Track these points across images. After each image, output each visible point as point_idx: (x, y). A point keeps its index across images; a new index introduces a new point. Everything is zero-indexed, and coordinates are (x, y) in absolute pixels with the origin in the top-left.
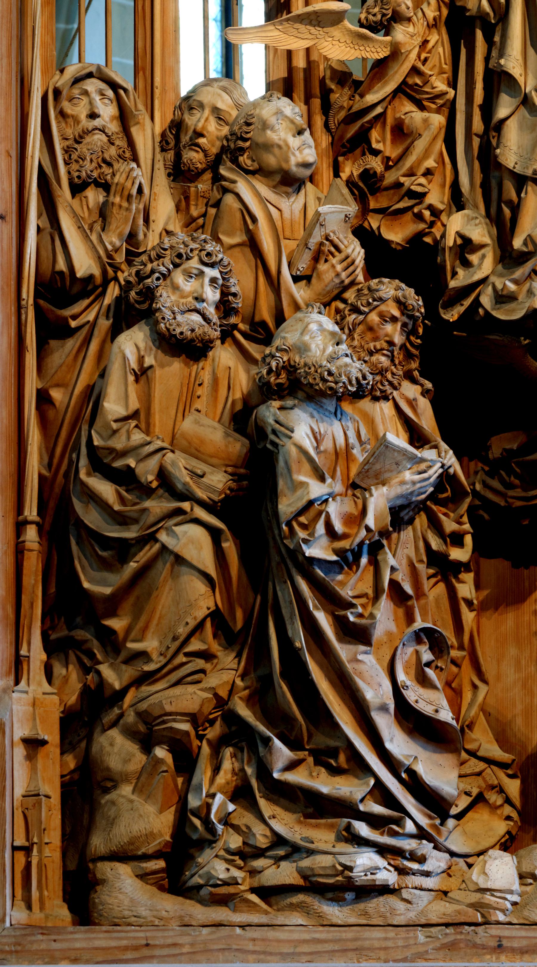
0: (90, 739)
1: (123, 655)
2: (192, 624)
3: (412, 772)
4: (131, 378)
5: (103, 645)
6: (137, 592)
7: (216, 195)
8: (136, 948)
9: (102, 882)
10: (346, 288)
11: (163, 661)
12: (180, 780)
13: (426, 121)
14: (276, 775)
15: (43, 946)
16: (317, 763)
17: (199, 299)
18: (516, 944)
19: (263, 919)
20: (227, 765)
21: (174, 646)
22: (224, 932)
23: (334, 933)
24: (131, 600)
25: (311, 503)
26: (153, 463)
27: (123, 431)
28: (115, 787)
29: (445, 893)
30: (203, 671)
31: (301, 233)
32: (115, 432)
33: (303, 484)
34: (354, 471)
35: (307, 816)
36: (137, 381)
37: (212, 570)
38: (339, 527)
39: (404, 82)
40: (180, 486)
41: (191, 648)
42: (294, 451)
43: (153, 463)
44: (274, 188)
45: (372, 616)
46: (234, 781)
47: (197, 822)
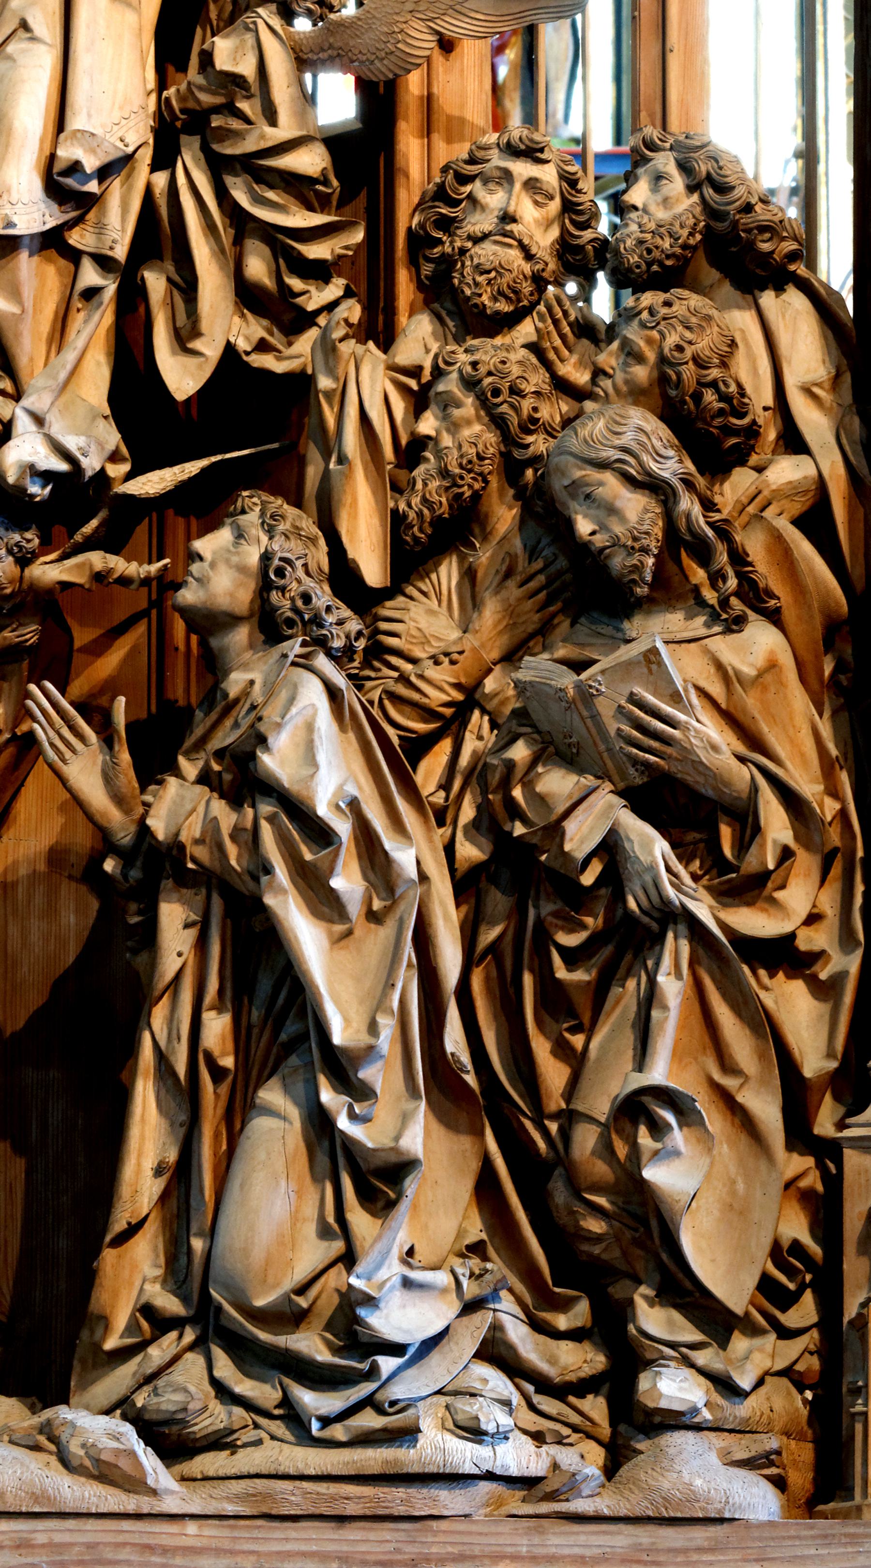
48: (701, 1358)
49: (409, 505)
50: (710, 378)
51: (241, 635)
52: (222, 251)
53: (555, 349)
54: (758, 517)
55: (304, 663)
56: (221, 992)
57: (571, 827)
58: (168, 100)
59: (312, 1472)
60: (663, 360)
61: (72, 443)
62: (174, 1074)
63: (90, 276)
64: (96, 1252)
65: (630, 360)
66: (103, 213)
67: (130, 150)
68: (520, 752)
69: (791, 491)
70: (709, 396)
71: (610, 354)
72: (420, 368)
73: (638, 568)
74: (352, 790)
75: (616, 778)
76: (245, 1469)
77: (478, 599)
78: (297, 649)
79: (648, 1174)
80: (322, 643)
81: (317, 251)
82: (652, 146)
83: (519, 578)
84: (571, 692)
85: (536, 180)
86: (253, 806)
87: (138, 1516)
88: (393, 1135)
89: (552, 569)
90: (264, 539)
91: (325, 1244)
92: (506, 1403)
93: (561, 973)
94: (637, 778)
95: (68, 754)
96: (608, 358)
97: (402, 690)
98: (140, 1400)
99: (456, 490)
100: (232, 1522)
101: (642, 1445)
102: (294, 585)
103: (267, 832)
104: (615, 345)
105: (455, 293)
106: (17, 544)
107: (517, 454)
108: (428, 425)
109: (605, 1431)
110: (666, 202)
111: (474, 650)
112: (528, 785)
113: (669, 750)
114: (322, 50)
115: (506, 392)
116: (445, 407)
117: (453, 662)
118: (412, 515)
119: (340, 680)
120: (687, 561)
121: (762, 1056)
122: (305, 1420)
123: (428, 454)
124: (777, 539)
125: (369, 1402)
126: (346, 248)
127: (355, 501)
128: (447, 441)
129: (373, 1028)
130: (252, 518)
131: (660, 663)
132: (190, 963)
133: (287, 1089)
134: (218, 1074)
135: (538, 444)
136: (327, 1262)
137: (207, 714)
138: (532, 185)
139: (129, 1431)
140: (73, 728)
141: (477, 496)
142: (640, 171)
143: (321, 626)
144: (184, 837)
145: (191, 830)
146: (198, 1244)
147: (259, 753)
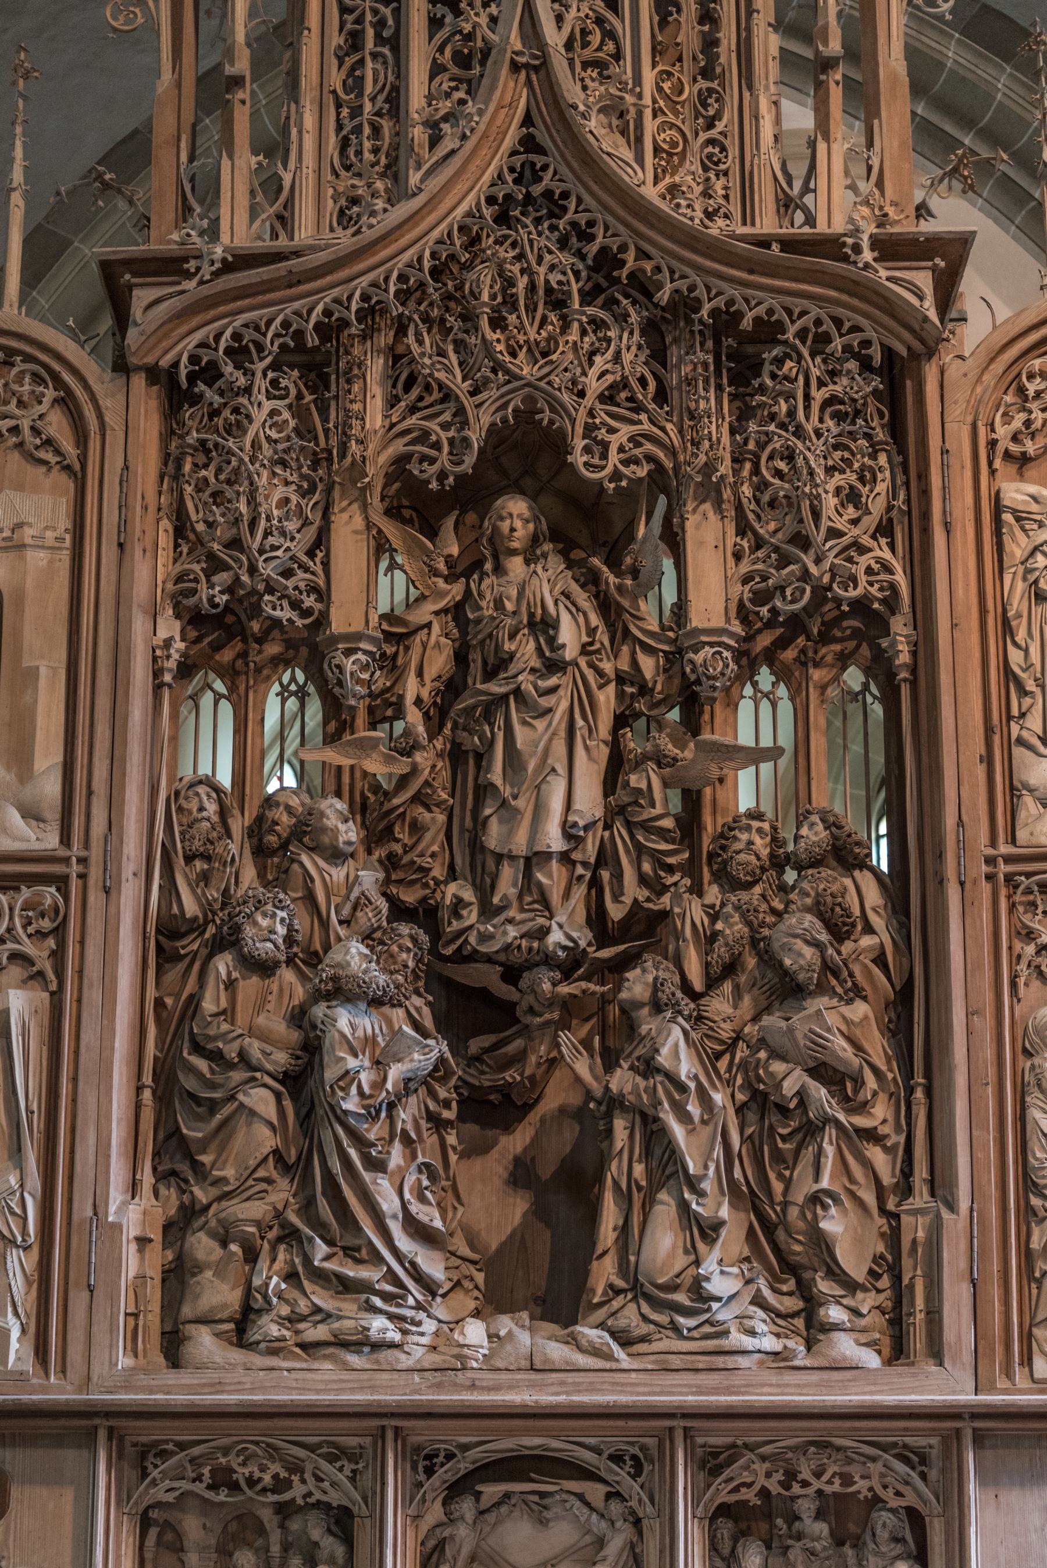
0: (183, 1239)
1: (210, 1180)
2: (260, 1158)
3: (413, 1264)
4: (222, 986)
5: (195, 1172)
6: (221, 1136)
7: (286, 864)
8: (212, 1385)
9: (189, 1338)
10: (374, 931)
11: (238, 1184)
12: (247, 1268)
13: (433, 819)
14: (316, 1263)
15: (145, 1383)
16: (346, 1255)
17: (272, 932)
18: (485, 1384)
19: (304, 1365)
20: (281, 1256)
21: (246, 1174)
22: (275, 1374)
23: (355, 1375)
24: (217, 1142)
25: (347, 1072)
26: (236, 1045)
27: (215, 1023)
28: (200, 1272)
29: (435, 1348)
30: (266, 1191)
31: (343, 892)
32: (210, 1023)
33: (342, 1059)
34: (378, 1052)
35: (338, 1293)
36: (226, 989)
37: (275, 1121)
38: (367, 1089)
39: (419, 791)
40: (254, 1061)
41: (257, 1175)
42: (337, 1035)
43: (236, 1045)
44: (326, 860)
45: (389, 1153)
46: (287, 1269)
47: (258, 1296)
48: (845, 1301)
51: (645, 1011)
54: (857, 959)
55: (673, 1020)
57: (786, 1084)
60: (818, 894)
61: (575, 935)
62: (621, 1189)
63: (580, 870)
66: (585, 845)
68: (762, 1055)
69: (870, 949)
70: (838, 909)
73: (810, 978)
74: (693, 1070)
79: (821, 1225)
80: (680, 1012)
82: (809, 812)
87: (611, 1370)
92: (764, 1321)
93: (780, 1145)
94: (812, 1064)
96: (793, 896)
97: (710, 1033)
101: (821, 1337)
105: (728, 875)
107: (757, 936)
108: (719, 926)
109: (805, 1334)
112: (766, 1069)
119: (688, 1027)
121: (867, 1176)
124: (866, 966)
125: (707, 1321)
128: (728, 932)
129: (706, 1167)
130: (650, 963)
134: (639, 1188)
135: (766, 932)
138: (760, 830)
139: (606, 1335)
141: (740, 954)
145: (628, 1088)
146: (632, 1258)
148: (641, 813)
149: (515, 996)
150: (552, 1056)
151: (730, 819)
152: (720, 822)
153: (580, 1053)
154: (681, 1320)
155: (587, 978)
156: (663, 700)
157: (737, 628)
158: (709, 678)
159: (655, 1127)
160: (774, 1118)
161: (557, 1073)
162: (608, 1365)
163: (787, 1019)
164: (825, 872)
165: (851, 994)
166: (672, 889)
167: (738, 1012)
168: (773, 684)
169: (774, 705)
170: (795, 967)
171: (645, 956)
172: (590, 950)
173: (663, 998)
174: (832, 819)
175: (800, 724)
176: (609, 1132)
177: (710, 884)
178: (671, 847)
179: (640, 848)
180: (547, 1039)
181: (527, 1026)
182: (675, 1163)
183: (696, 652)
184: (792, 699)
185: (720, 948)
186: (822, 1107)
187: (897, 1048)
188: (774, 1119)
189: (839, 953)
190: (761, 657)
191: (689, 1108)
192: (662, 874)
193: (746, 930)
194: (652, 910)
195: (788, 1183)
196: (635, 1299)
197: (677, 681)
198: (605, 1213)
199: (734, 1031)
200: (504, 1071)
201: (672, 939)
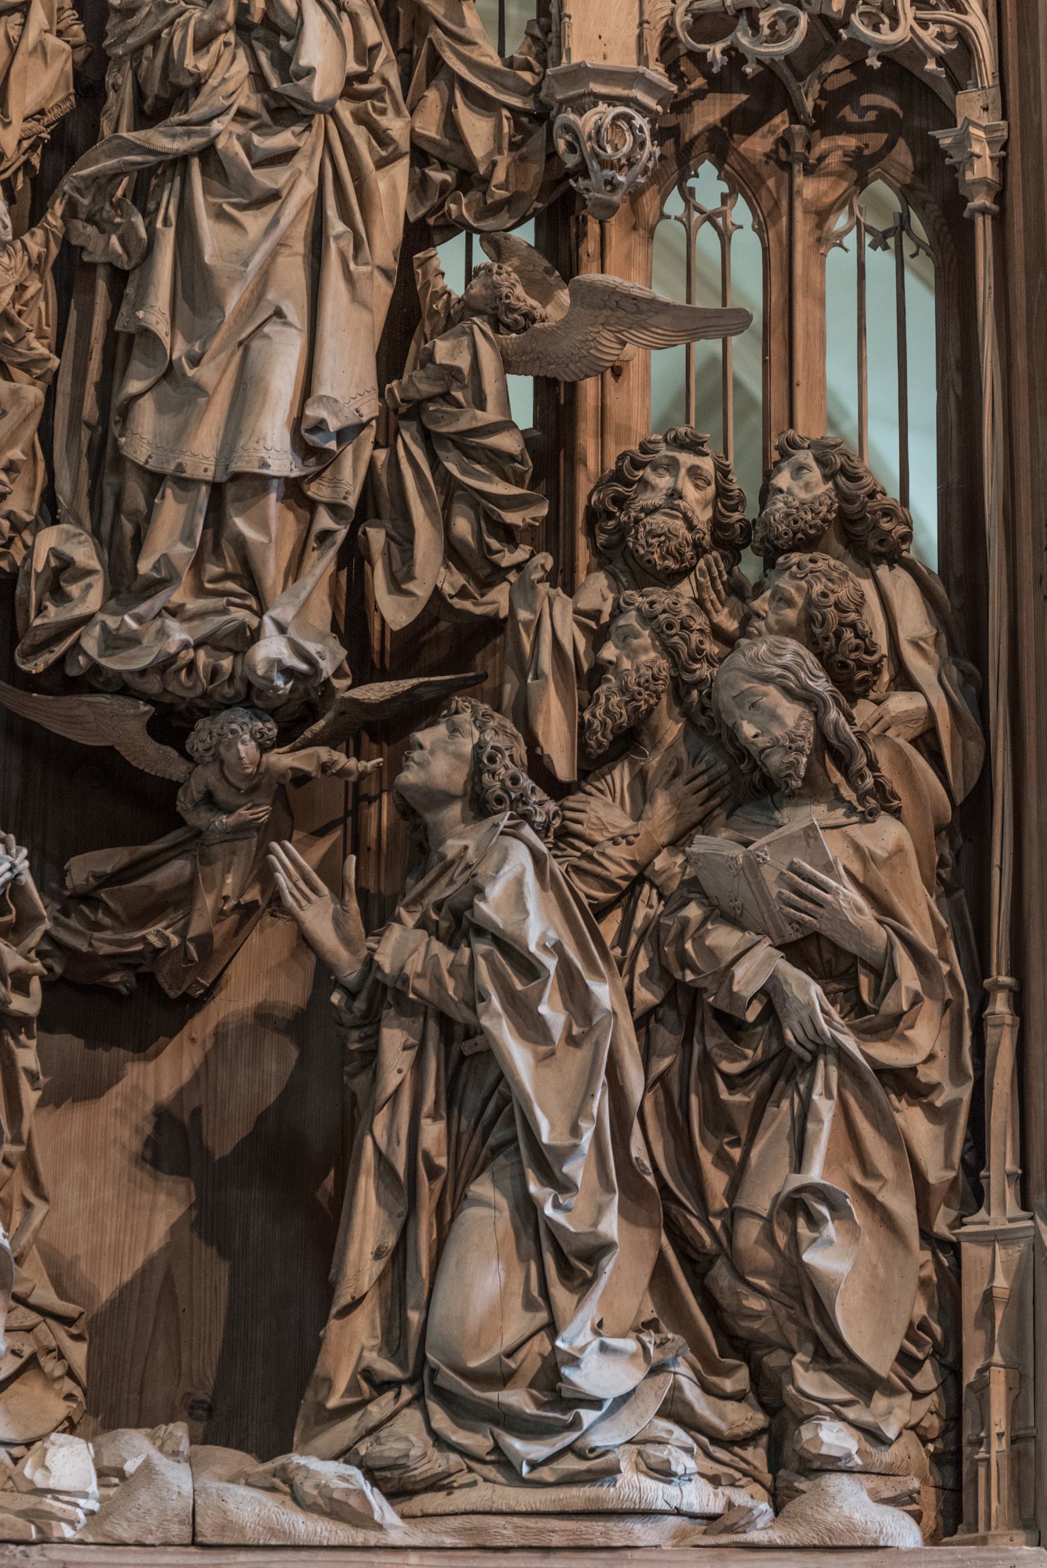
49: (594, 715)
50: (849, 620)
51: (455, 810)
52: (435, 511)
53: (712, 601)
55: (511, 832)
56: (436, 1102)
57: (740, 972)
58: (391, 390)
59: (523, 1509)
61: (312, 648)
64: (324, 1322)
65: (782, 604)
66: (338, 470)
67: (365, 419)
68: (693, 911)
71: (764, 600)
72: (599, 612)
73: (794, 765)
74: (552, 934)
75: (774, 935)
76: (463, 1507)
77: (649, 794)
78: (505, 822)
80: (527, 817)
81: (513, 518)
82: (793, 445)
83: (685, 777)
84: (741, 860)
85: (698, 467)
86: (469, 945)
87: (366, 1548)
88: (590, 1222)
89: (713, 771)
90: (476, 733)
91: (530, 1315)
94: (792, 935)
95: (304, 903)
96: (760, 604)
97: (585, 864)
98: (363, 1449)
99: (634, 703)
100: (449, 1553)
102: (502, 770)
103: (482, 965)
104: (768, 594)
106: (260, 731)
107: (686, 677)
108: (609, 652)
110: (807, 486)
111: (648, 833)
112: (699, 940)
113: (821, 911)
114: (524, 353)
115: (678, 627)
116: (625, 638)
117: (629, 843)
118: (597, 723)
119: (543, 847)
120: (829, 764)
122: (516, 1464)
123: (610, 676)
126: (534, 519)
127: (548, 712)
128: (626, 664)
129: (575, 1131)
130: (466, 716)
131: (817, 838)
132: (408, 1078)
133: (495, 1183)
134: (433, 1172)
135: (703, 670)
136: (532, 1329)
137: (418, 881)
138: (694, 472)
139: (357, 1474)
140: (308, 882)
141: (650, 711)
142: (784, 464)
143: (525, 803)
144: (408, 970)
145: (415, 965)
146: (414, 1317)
147: (476, 901)
148: (456, 418)
149: (172, 766)
150: (248, 898)
151: (635, 448)
152: (613, 452)
153: (315, 890)
154: (517, 1445)
155: (330, 739)
156: (506, 204)
157: (656, 73)
158: (604, 164)
159: (467, 1048)
160: (714, 1040)
161: (255, 938)
162: (359, 1537)
163: (747, 844)
164: (825, 562)
165: (872, 803)
166: (512, 577)
167: (643, 827)
168: (724, 198)
169: (725, 237)
170: (762, 741)
171: (458, 701)
172: (340, 684)
173: (493, 785)
174: (839, 461)
175: (775, 280)
176: (371, 1055)
177: (589, 572)
178: (515, 491)
179: (449, 487)
180: (241, 862)
181: (199, 834)
182: (512, 1121)
183: (581, 111)
184: (761, 229)
185: (608, 692)
186: (813, 1021)
187: (955, 915)
188: (711, 1042)
189: (850, 720)
190: (701, 145)
191: (543, 1009)
192: (495, 544)
193: (664, 663)
194: (470, 614)
195: (737, 1174)
196: (418, 1399)
197: (535, 169)
198: (358, 1220)
199: (633, 863)
200: (143, 926)
201: (510, 674)
